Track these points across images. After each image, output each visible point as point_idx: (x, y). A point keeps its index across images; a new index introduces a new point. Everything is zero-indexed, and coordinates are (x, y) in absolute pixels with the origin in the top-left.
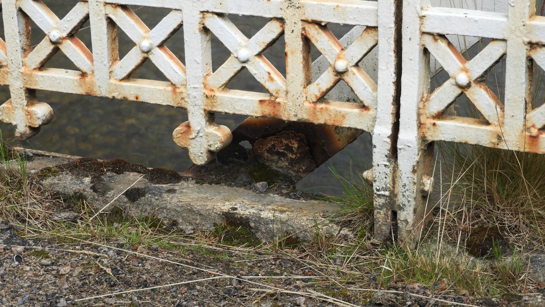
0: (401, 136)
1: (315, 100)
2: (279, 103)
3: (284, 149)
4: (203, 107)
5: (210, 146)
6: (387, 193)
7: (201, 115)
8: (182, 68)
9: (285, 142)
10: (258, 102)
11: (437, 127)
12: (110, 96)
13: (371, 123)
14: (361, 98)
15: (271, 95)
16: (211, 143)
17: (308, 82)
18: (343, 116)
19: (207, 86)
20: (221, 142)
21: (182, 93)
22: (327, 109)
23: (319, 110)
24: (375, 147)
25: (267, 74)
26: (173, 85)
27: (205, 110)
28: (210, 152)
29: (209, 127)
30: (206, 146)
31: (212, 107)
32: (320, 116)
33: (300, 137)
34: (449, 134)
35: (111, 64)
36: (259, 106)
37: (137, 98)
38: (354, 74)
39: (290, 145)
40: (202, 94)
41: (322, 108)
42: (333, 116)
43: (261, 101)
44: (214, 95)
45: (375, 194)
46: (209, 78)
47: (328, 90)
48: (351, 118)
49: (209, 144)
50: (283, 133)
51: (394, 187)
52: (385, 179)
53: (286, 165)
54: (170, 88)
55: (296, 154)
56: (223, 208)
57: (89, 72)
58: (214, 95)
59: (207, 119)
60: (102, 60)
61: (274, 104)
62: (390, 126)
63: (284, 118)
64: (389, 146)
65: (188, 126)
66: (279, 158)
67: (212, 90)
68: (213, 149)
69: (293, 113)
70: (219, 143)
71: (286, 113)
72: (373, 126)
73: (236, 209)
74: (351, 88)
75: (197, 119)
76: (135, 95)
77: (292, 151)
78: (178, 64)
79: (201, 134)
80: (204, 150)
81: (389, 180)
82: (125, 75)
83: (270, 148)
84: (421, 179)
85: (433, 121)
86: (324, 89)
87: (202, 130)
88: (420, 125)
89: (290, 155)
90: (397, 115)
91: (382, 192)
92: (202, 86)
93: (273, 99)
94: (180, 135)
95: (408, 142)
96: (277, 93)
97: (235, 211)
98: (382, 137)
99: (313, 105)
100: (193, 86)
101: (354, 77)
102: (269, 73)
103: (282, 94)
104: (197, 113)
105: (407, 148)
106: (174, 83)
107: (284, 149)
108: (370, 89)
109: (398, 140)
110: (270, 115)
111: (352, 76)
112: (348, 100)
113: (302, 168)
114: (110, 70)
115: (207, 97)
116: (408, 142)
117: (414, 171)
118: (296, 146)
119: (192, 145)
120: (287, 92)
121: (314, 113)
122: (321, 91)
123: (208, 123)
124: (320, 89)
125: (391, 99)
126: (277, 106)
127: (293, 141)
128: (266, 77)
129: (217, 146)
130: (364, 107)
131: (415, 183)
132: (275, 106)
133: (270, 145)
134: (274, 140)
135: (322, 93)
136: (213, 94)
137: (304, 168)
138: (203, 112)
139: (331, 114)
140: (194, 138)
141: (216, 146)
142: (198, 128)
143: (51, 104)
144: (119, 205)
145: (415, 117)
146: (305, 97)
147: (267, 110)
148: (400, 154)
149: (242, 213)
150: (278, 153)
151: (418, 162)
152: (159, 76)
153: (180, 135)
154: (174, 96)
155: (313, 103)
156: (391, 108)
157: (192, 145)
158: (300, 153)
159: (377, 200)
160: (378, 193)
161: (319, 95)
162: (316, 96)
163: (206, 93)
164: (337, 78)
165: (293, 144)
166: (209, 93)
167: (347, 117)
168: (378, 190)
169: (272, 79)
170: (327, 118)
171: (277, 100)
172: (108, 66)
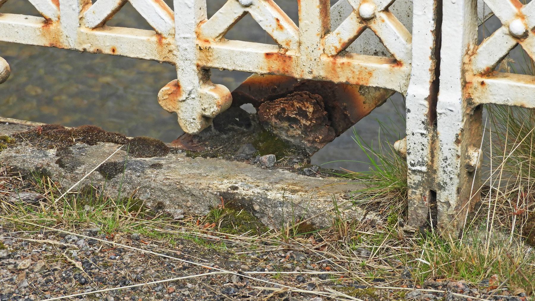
0: (442, 97)
1: (334, 53)
2: (290, 57)
3: (296, 114)
4: (195, 62)
6: (424, 169)
7: (193, 72)
8: (170, 13)
9: (297, 105)
10: (264, 56)
11: (487, 86)
12: (81, 49)
13: (404, 81)
14: (392, 51)
15: (280, 47)
17: (327, 31)
18: (370, 74)
19: (201, 36)
20: (218, 106)
21: (169, 44)
22: (349, 64)
23: (339, 66)
24: (409, 111)
25: (275, 21)
26: (158, 34)
27: (198, 66)
28: (205, 118)
29: (203, 87)
30: (200, 111)
31: (207, 62)
32: (341, 73)
33: (316, 99)
34: (502, 95)
35: (81, 8)
36: (265, 60)
37: (114, 51)
38: (383, 21)
39: (304, 109)
40: (195, 46)
41: (343, 63)
42: (357, 73)
43: (268, 55)
44: (210, 47)
45: (410, 169)
46: (202, 26)
47: (351, 41)
48: (380, 75)
49: (203, 107)
50: (295, 95)
51: (432, 161)
52: (421, 151)
53: (299, 134)
54: (155, 39)
55: (311, 120)
56: (220, 187)
57: (54, 19)
58: (210, 47)
59: (201, 76)
60: (70, 3)
61: (284, 58)
62: (428, 86)
63: (297, 76)
64: (426, 111)
65: (178, 86)
66: (290, 125)
67: (207, 41)
68: (207, 113)
69: (307, 70)
70: (215, 106)
71: (299, 69)
72: (407, 86)
73: (236, 188)
74: (380, 39)
75: (188, 77)
76: (111, 47)
77: (306, 117)
78: (164, 8)
79: (192, 96)
80: (196, 115)
81: (427, 152)
82: (98, 22)
83: (279, 113)
84: (467, 151)
85: (481, 79)
86: (346, 39)
87: (194, 90)
88: (465, 84)
89: (304, 122)
90: (437, 72)
91: (418, 168)
92: (195, 36)
93: (282, 52)
94: (167, 97)
95: (450, 105)
96: (287, 44)
97: (236, 191)
98: (418, 99)
99: (332, 59)
100: (183, 36)
101: (383, 24)
102: (278, 20)
103: (294, 46)
104: (189, 70)
105: (449, 112)
106: (159, 32)
107: (296, 114)
108: (403, 40)
109: (438, 103)
110: (278, 71)
111: (380, 24)
112: (376, 54)
113: (319, 138)
114: (81, 16)
115: (200, 49)
116: (450, 105)
117: (458, 142)
118: (311, 110)
119: (182, 109)
120: (300, 44)
121: (334, 69)
122: (342, 41)
123: (201, 82)
124: (341, 40)
125: (429, 52)
126: (287, 60)
127: (308, 104)
128: (274, 24)
129: (212, 110)
130: (396, 62)
131: (458, 156)
132: (285, 61)
133: (278, 109)
134: (283, 103)
135: (343, 44)
136: (207, 45)
137: (321, 137)
138: (195, 68)
139: (355, 70)
140: (184, 101)
141: (212, 110)
142: (190, 88)
143: (7, 58)
144: (92, 183)
145: (459, 75)
146: (322, 49)
147: (276, 66)
148: (440, 120)
149: (244, 193)
150: (289, 119)
151: (462, 130)
152: (142, 24)
153: (167, 97)
154: (160, 48)
155: (332, 56)
156: (429, 64)
157: (182, 109)
158: (316, 119)
159: (411, 177)
160: (413, 168)
161: (339, 47)
162: (336, 48)
163: (200, 45)
164: (362, 25)
165: (308, 108)
167: (374, 74)
168: (413, 165)
169: (281, 27)
170: (350, 75)
171: (288, 53)
172: (78, 10)
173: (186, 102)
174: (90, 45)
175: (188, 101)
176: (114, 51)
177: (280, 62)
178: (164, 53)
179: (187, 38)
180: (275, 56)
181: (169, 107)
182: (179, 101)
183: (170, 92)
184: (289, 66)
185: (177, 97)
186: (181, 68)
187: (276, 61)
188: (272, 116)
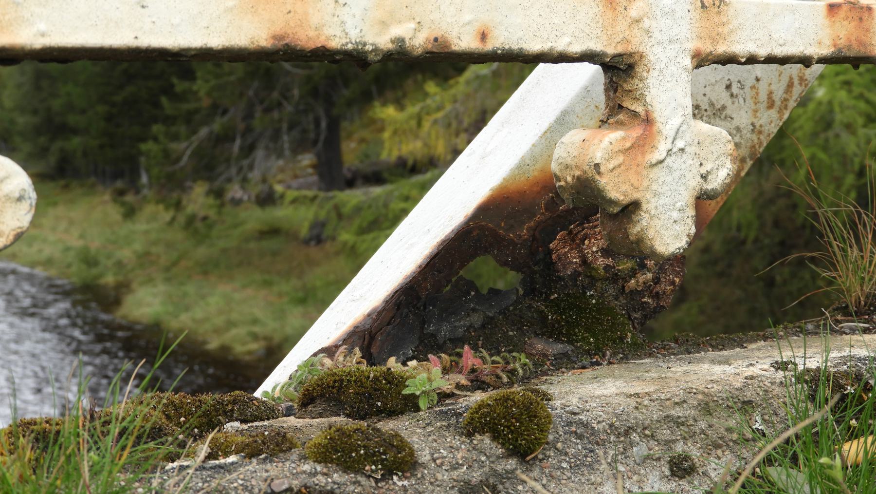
4: (692, 45)
5: (704, 177)
16: (708, 167)
36: (827, 22)
49: (703, 171)
65: (648, 121)
87: (684, 127)
94: (621, 158)
110: (849, 47)
113: (673, 283)
119: (654, 187)
126: (865, 16)
132: (861, 19)
142: (676, 121)
154: (609, 14)
157: (654, 187)
173: (665, 164)
175: (669, 160)
176: (483, 37)
177: (853, 24)
178: (618, 28)
180: (845, 8)
181: (624, 188)
182: (653, 166)
183: (628, 144)
184: (868, 30)
185: (643, 154)
186: (657, 68)
187: (846, 23)
188: (597, 252)
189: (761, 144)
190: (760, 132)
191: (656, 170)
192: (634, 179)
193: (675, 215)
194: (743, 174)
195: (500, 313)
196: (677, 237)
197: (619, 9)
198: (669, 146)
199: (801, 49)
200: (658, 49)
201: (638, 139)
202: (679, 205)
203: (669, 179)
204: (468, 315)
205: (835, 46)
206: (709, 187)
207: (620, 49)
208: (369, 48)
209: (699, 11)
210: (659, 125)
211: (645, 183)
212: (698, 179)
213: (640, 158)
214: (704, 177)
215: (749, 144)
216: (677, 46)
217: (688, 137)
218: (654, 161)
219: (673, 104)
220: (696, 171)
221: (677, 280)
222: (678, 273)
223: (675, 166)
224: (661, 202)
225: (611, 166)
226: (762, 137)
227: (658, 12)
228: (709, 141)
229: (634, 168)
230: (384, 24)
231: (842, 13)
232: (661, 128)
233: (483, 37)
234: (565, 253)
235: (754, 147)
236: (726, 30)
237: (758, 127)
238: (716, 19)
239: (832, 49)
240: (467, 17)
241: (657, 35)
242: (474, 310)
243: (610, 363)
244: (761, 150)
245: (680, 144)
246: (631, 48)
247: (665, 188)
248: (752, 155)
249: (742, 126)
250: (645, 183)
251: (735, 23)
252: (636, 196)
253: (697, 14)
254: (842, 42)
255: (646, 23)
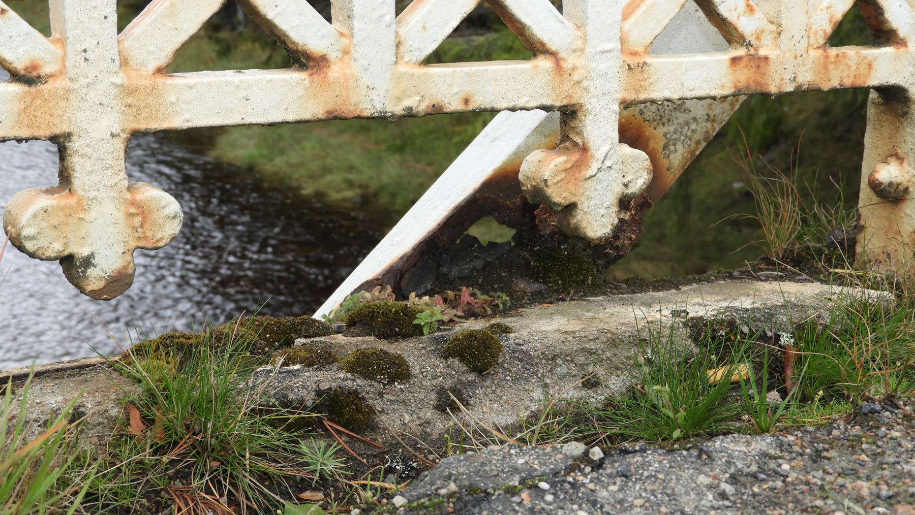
2: (766, 58)
4: (620, 96)
5: (626, 185)
12: (399, 110)
16: (629, 178)
18: (870, 66)
21: (574, 69)
31: (637, 91)
36: (730, 71)
43: (735, 61)
44: (645, 63)
49: (625, 180)
61: (759, 62)
63: (773, 89)
65: (584, 149)
69: (788, 76)
71: (777, 77)
94: (563, 175)
96: (758, 38)
99: (821, 51)
100: (600, 48)
113: (630, 239)
115: (630, 68)
119: (587, 193)
121: (826, 68)
124: (832, 18)
126: (763, 64)
132: (758, 67)
142: (605, 149)
153: (563, 175)
154: (558, 79)
157: (587, 193)
166: (633, 61)
167: (875, 65)
173: (596, 177)
174: (418, 98)
175: (599, 175)
176: (467, 101)
177: (751, 70)
178: (564, 89)
179: (609, 51)
180: (745, 60)
181: (564, 195)
182: (586, 179)
183: (568, 166)
184: (764, 74)
185: (580, 171)
186: (593, 113)
187: (746, 70)
189: (714, 130)
190: (714, 121)
191: (589, 182)
192: (572, 189)
193: (603, 211)
194: (697, 153)
195: (497, 259)
196: (603, 226)
197: (565, 75)
198: (599, 165)
199: (707, 92)
200: (594, 101)
201: (576, 161)
202: (606, 204)
203: (599, 187)
204: (472, 261)
205: (735, 87)
206: (630, 192)
207: (565, 102)
208: (389, 114)
209: (626, 71)
210: (592, 152)
211: (581, 191)
212: (621, 186)
213: (577, 174)
214: (626, 185)
215: (703, 130)
216: (608, 97)
217: (614, 158)
218: (587, 176)
219: (604, 136)
220: (620, 181)
221: (634, 236)
222: (635, 231)
223: (604, 178)
224: (593, 203)
225: (555, 181)
226: (715, 125)
227: (594, 75)
228: (630, 160)
229: (573, 181)
230: (399, 99)
231: (743, 64)
232: (594, 153)
233: (467, 101)
234: (546, 218)
235: (708, 132)
236: (647, 83)
237: (712, 116)
238: (640, 76)
239: (733, 90)
240: (456, 90)
241: (593, 91)
242: (476, 257)
243: (572, 299)
244: (714, 134)
245: (608, 163)
246: (574, 101)
247: (596, 193)
248: (705, 140)
249: (698, 117)
250: (581, 191)
251: (654, 77)
252: (573, 199)
253: (624, 74)
254: (741, 85)
255: (585, 83)
